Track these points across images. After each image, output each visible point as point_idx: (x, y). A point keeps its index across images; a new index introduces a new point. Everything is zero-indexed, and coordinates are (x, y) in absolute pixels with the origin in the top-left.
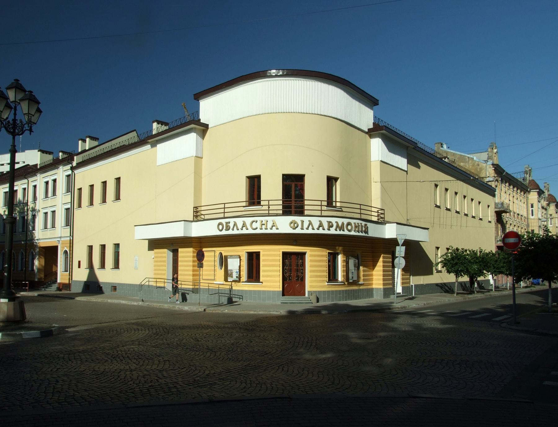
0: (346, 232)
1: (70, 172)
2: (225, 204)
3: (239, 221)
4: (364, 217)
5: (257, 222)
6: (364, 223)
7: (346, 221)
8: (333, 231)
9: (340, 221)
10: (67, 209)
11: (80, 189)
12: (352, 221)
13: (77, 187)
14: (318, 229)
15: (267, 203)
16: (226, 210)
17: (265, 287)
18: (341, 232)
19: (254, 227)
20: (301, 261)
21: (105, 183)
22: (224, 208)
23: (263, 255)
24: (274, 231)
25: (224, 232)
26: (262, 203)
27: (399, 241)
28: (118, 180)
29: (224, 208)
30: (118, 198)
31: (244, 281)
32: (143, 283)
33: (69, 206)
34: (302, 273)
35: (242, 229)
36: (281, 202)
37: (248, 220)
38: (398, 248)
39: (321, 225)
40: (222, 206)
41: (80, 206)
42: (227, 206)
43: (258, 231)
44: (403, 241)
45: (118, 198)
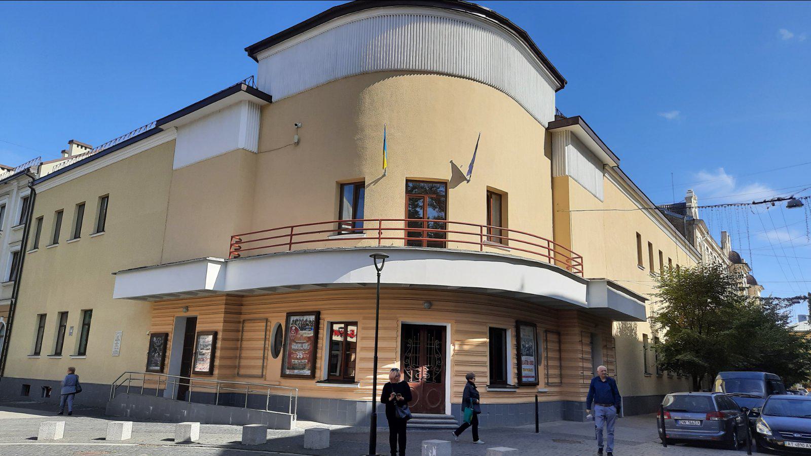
1: (28, 192)
2: (292, 227)
10: (15, 254)
11: (40, 219)
13: (36, 215)
15: (376, 225)
21: (81, 207)
22: (291, 235)
26: (366, 225)
28: (104, 199)
29: (291, 235)
30: (100, 228)
31: (322, 379)
32: (118, 383)
33: (18, 248)
34: (439, 367)
36: (402, 225)
40: (288, 231)
41: (36, 247)
42: (296, 230)
45: (100, 228)
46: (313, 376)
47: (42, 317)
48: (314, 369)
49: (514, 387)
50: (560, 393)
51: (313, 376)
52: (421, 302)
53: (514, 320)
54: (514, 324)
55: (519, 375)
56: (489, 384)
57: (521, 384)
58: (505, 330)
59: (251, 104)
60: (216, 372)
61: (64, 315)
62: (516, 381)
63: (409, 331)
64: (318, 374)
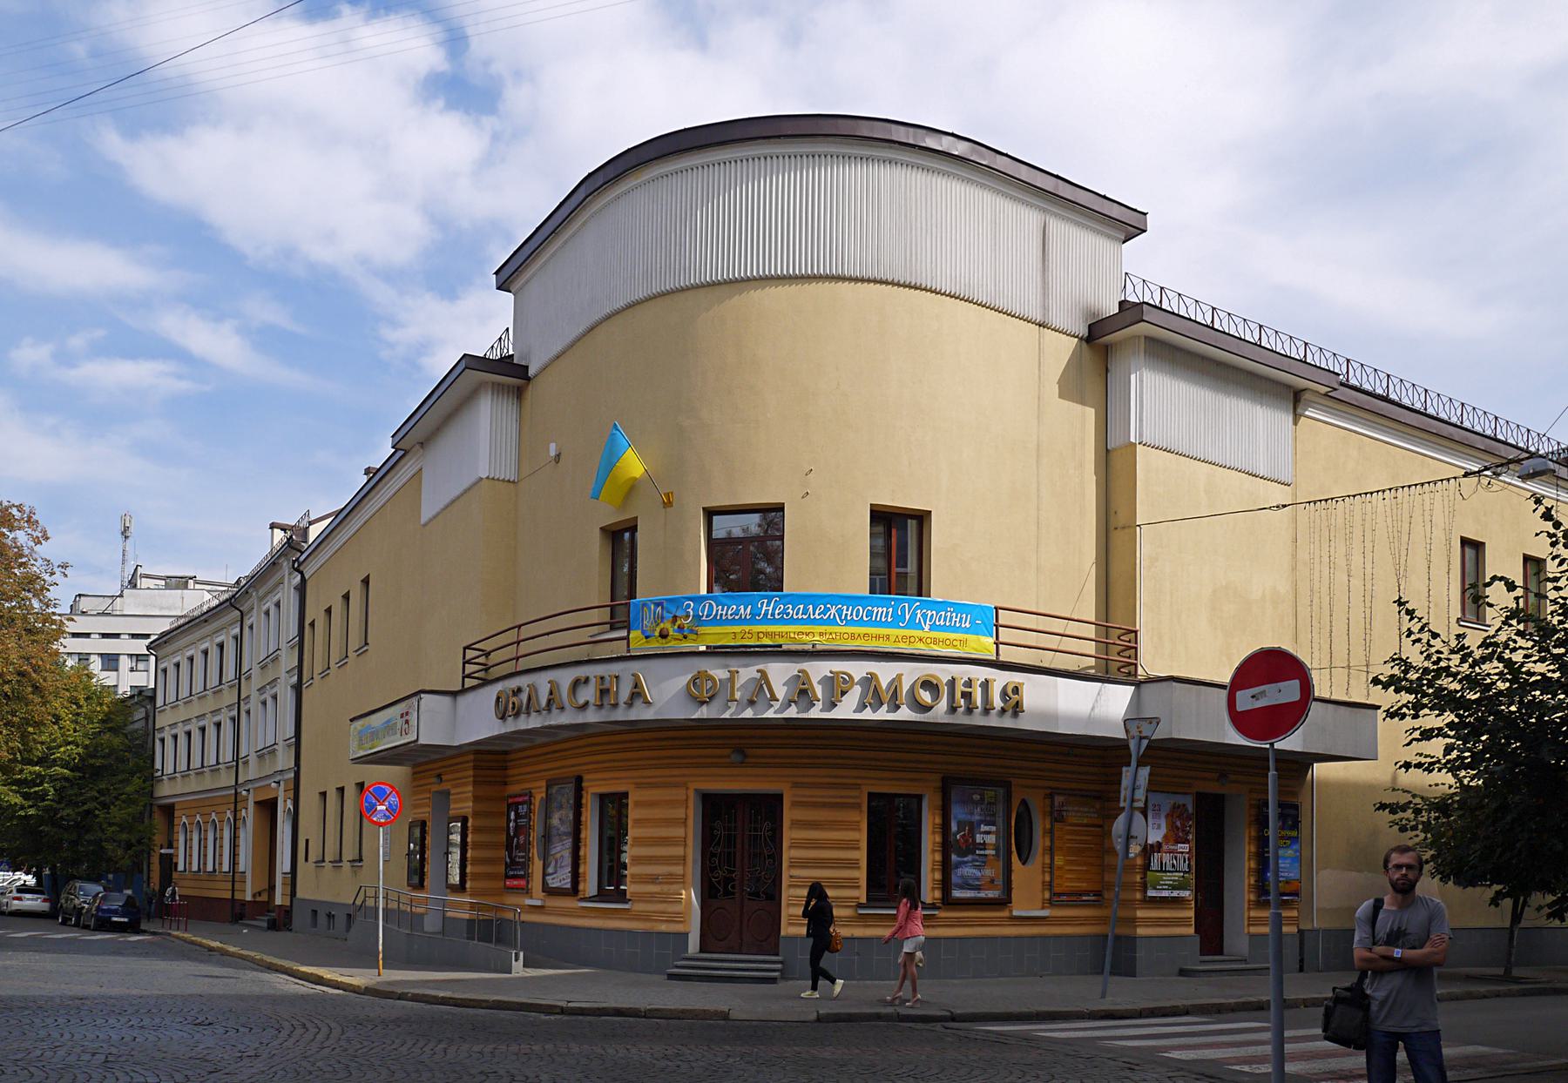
0: (905, 714)
3: (542, 682)
4: (1007, 654)
5: (587, 680)
6: (1001, 679)
7: (910, 673)
8: (846, 710)
9: (885, 672)
12: (943, 673)
14: (789, 702)
16: (525, 648)
17: (639, 917)
18: (883, 714)
19: (581, 701)
20: (767, 825)
23: (637, 804)
24: (640, 713)
25: (511, 726)
27: (1132, 745)
35: (549, 710)
37: (565, 678)
38: (1127, 774)
39: (802, 693)
42: (526, 632)
43: (591, 716)
44: (1145, 742)
46: (574, 891)
47: (324, 794)
48: (576, 876)
49: (933, 906)
50: (1103, 921)
51: (574, 891)
52: (727, 752)
53: (938, 777)
54: (939, 784)
55: (946, 885)
56: (863, 900)
57: (948, 902)
58: (919, 798)
59: (498, 389)
60: (468, 885)
61: (341, 790)
62: (938, 894)
63: (715, 807)
64: (581, 887)
